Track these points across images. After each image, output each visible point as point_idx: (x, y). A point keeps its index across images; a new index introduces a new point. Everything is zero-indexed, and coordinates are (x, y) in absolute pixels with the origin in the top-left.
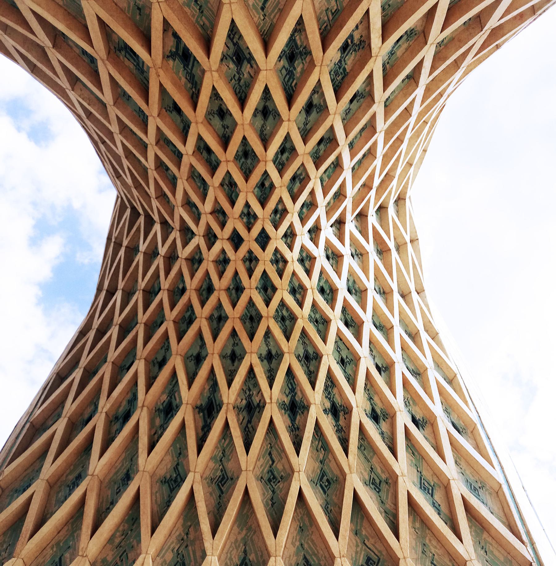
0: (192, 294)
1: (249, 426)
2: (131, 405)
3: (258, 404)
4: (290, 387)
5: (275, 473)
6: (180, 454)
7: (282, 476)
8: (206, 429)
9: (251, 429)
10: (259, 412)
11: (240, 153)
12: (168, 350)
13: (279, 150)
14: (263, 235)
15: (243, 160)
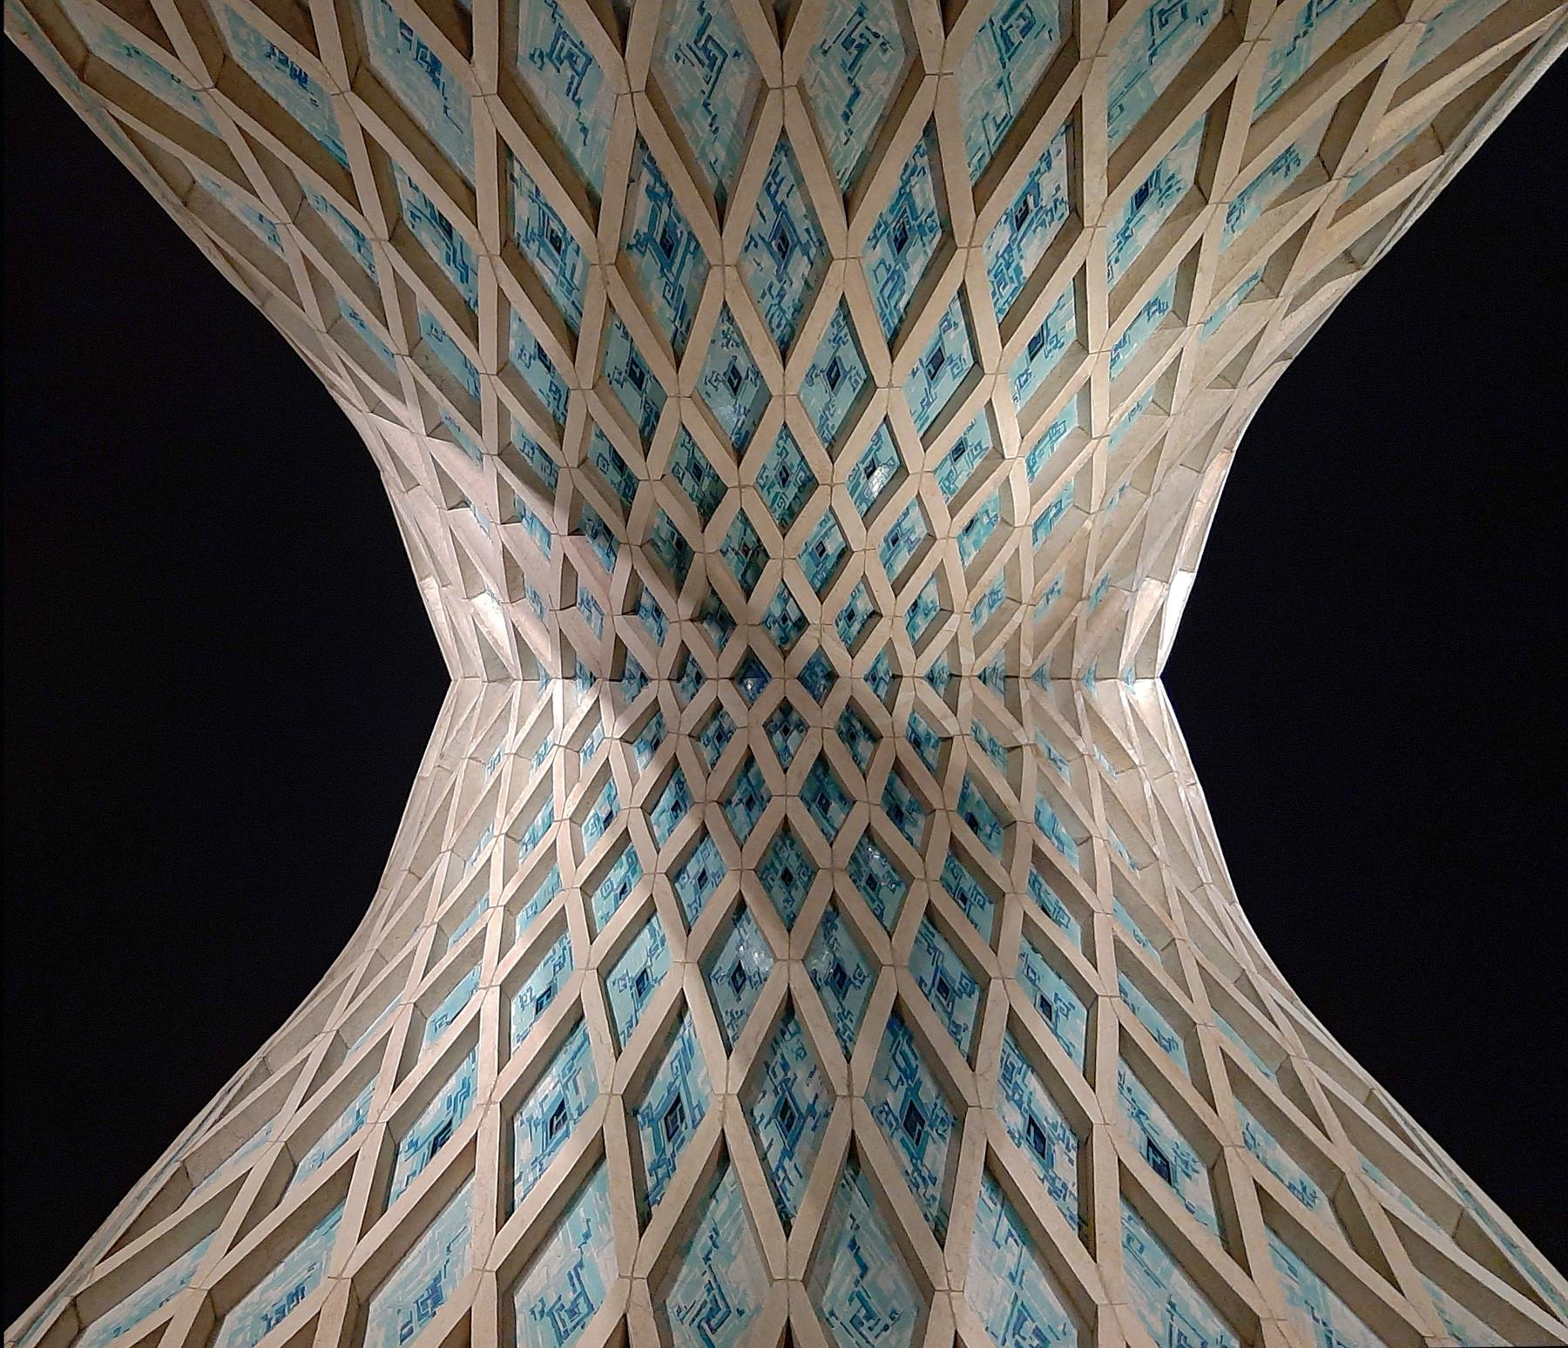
0: (632, 820)
1: (786, 1163)
2: (455, 1110)
3: (811, 1109)
4: (903, 1065)
5: (873, 1304)
6: (587, 1236)
7: (894, 1312)
8: (661, 1172)
9: (793, 1175)
10: (814, 1129)
11: (772, 473)
12: (561, 966)
13: (862, 467)
14: (818, 669)
15: (777, 488)
